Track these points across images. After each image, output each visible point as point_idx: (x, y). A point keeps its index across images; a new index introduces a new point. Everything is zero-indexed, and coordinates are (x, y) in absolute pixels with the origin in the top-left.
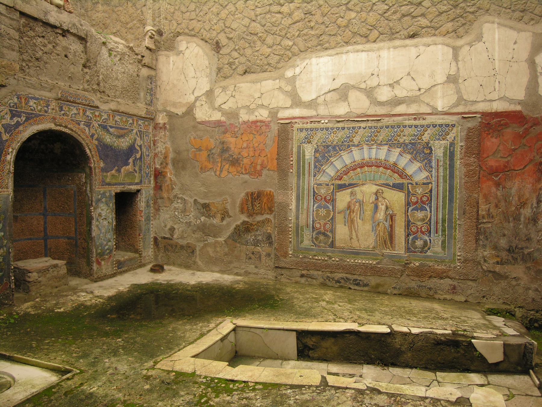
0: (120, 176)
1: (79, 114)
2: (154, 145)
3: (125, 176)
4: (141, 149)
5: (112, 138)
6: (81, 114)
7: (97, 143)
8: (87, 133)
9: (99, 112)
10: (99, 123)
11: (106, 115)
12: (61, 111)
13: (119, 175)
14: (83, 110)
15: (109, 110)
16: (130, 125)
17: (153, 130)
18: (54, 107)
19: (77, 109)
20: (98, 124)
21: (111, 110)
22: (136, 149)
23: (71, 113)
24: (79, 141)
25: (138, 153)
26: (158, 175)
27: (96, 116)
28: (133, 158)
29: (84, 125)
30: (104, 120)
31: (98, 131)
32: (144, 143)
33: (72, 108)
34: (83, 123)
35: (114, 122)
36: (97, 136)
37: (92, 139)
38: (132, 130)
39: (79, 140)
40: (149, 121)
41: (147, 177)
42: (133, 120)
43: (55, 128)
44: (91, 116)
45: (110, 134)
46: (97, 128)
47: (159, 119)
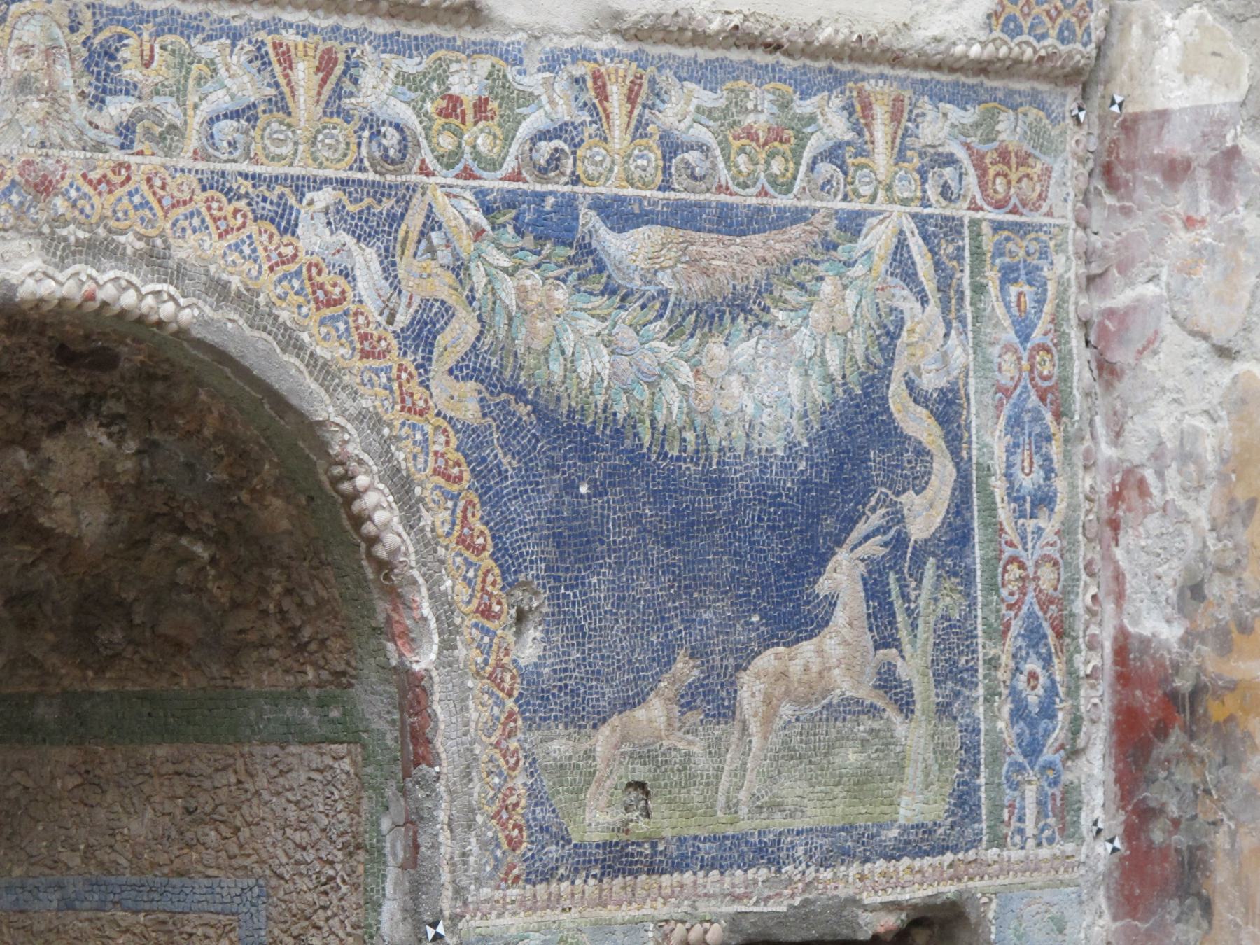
0: (731, 760)
1: (280, 105)
2: (1106, 370)
3: (786, 754)
4: (955, 440)
5: (626, 336)
6: (305, 105)
7: (470, 412)
8: (372, 307)
9: (484, 65)
10: (493, 182)
11: (561, 85)
12: (98, 101)
13: (716, 749)
14: (326, 65)
15: (594, 30)
16: (826, 169)
17: (1086, 198)
18: (37, 59)
19: (260, 58)
20: (480, 194)
21: (614, 23)
22: (889, 434)
23: (206, 109)
24: (281, 404)
25: (919, 483)
26: (1162, 731)
27: (455, 101)
28: (873, 548)
29: (336, 217)
30: (546, 147)
31: (479, 277)
32: (984, 365)
33: (209, 50)
34: (324, 197)
35: (655, 156)
36: (473, 328)
37: (423, 366)
38: (852, 225)
39: (282, 386)
40: (1036, 100)
41: (1032, 750)
42: (859, 113)
43: (47, 288)
44: (407, 115)
45: (610, 291)
46: (466, 245)
47: (1147, 59)
